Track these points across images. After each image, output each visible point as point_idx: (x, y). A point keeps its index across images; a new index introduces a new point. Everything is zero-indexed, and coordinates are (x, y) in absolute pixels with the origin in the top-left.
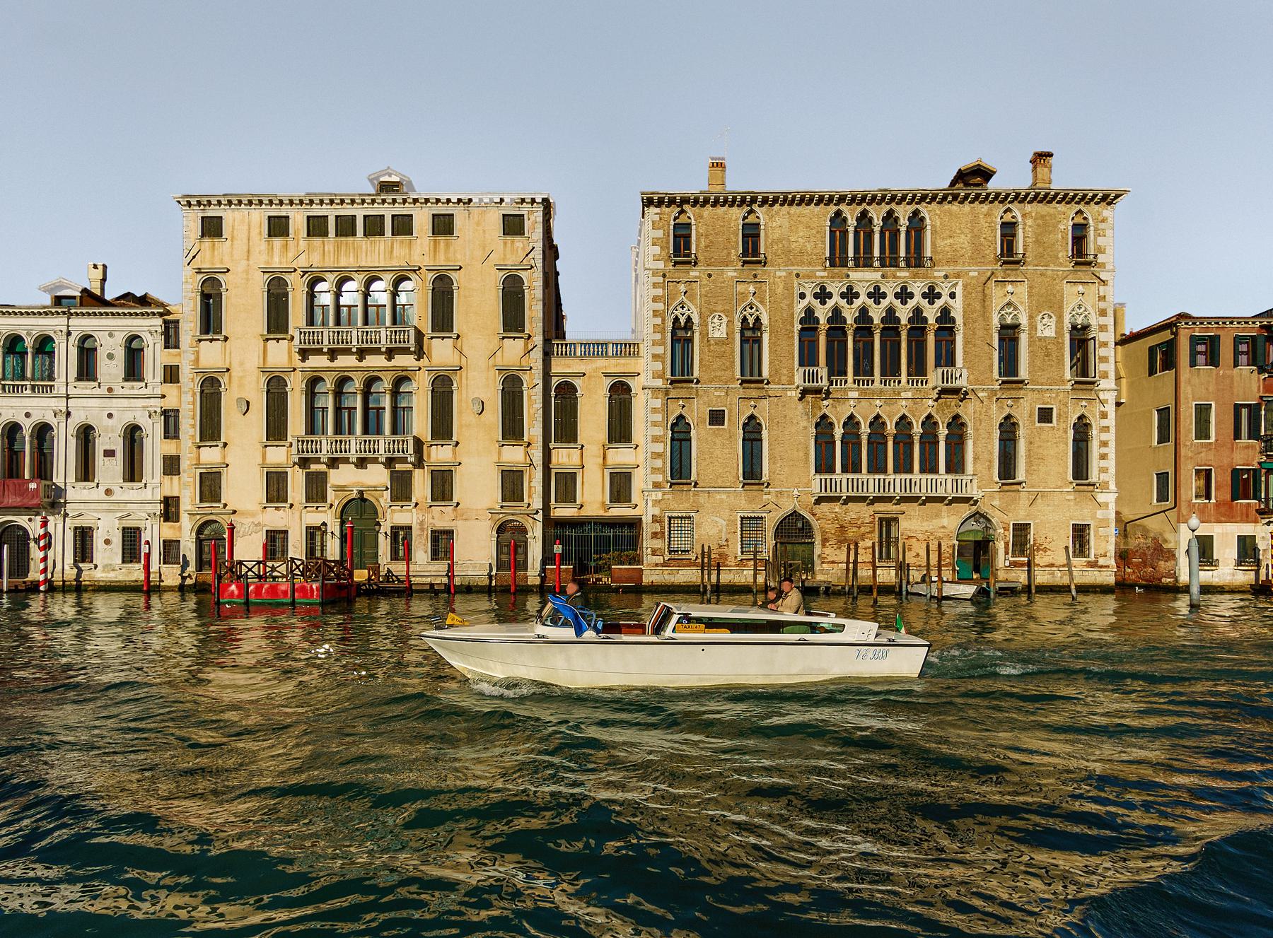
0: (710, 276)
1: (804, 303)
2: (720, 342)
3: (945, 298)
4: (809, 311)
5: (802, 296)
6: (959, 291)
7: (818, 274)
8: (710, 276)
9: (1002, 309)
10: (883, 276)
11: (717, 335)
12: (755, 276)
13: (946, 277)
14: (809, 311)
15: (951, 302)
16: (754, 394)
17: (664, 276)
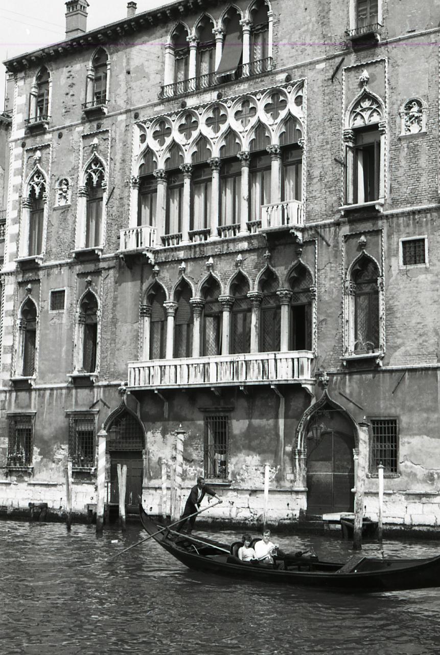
0: (60, 136)
1: (144, 146)
2: (66, 209)
3: (292, 107)
4: (148, 153)
5: (143, 138)
6: (304, 93)
7: (157, 109)
8: (60, 136)
9: (358, 104)
10: (219, 96)
11: (63, 203)
12: (99, 127)
13: (288, 79)
14: (148, 153)
15: (296, 111)
16: (91, 267)
17: (23, 145)
